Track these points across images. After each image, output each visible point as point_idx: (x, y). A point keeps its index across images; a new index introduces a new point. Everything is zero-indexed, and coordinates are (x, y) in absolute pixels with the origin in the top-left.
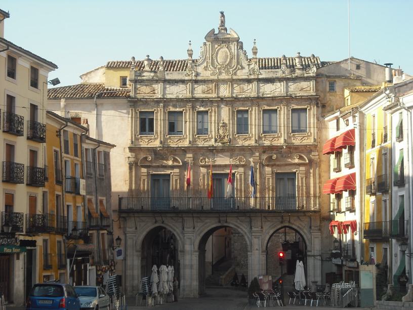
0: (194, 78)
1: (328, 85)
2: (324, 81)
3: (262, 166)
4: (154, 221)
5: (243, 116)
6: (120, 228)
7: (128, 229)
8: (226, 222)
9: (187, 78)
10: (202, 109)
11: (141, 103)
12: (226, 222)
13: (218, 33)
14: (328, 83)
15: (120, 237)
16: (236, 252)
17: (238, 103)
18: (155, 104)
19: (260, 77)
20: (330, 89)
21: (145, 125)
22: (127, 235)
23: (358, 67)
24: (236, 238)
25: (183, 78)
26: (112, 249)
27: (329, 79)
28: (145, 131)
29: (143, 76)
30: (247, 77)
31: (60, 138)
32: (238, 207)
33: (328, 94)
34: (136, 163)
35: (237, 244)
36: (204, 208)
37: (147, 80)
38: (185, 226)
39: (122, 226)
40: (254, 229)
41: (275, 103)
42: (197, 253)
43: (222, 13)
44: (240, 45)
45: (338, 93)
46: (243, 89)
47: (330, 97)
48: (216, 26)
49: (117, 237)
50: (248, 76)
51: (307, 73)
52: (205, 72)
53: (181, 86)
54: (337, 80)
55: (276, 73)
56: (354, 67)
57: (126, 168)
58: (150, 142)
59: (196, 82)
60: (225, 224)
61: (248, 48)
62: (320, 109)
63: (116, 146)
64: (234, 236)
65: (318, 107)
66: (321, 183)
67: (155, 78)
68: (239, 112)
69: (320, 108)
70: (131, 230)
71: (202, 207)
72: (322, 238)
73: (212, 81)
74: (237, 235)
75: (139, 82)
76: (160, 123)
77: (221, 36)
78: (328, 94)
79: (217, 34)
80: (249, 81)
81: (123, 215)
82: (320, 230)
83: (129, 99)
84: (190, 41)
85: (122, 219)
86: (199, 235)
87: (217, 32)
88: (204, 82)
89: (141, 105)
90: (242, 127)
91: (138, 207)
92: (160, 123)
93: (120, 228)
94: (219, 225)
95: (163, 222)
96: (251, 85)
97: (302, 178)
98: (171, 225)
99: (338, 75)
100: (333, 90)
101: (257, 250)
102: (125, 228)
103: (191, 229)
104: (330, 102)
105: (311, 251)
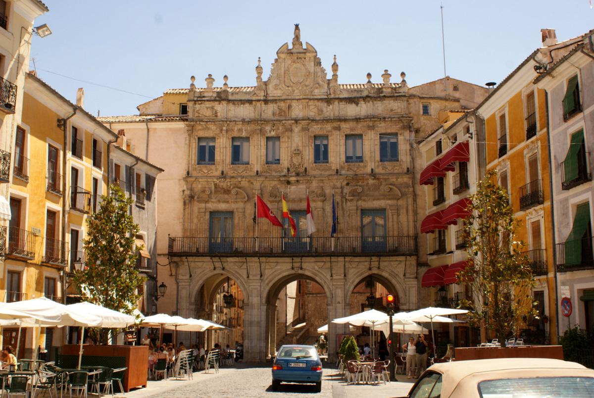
0: (262, 98)
1: (421, 108)
2: (417, 103)
3: (345, 201)
4: (212, 267)
5: (321, 142)
6: (171, 275)
7: (180, 277)
8: (301, 268)
9: (254, 98)
10: (273, 134)
11: (200, 127)
12: (301, 268)
13: (293, 49)
14: (421, 106)
15: (164, 284)
16: (310, 312)
17: (315, 126)
18: (216, 129)
19: (341, 96)
20: (424, 113)
21: (205, 154)
22: (180, 284)
23: (456, 89)
24: (310, 298)
25: (250, 99)
26: (153, 298)
27: (422, 101)
28: (205, 161)
29: (204, 97)
30: (326, 97)
31: (65, 130)
32: (316, 249)
33: (422, 118)
34: (192, 197)
35: (311, 305)
36: (274, 251)
37: (208, 101)
38: (251, 273)
39: (174, 273)
40: (335, 277)
41: (359, 127)
42: (265, 307)
43: (297, 26)
44: (318, 63)
45: (433, 117)
46: (322, 111)
47: (425, 121)
48: (289, 39)
49: (161, 283)
50: (327, 96)
51: (396, 93)
52: (275, 92)
53: (248, 108)
54: (431, 101)
55: (360, 93)
56: (451, 88)
57: (180, 205)
58: (209, 172)
59: (266, 101)
60: (300, 272)
61: (327, 65)
62: (413, 134)
63: (163, 171)
64: (308, 297)
65: (410, 131)
66: (417, 222)
67: (217, 99)
68: (316, 137)
69: (413, 133)
70: (184, 278)
71: (272, 249)
72: (418, 287)
73: (284, 100)
74: (311, 296)
75: (199, 104)
76: (223, 150)
77: (293, 51)
78: (422, 118)
79: (290, 50)
80: (329, 101)
81: (175, 259)
82: (416, 278)
83: (185, 123)
84: (259, 58)
85: (175, 265)
86: (268, 284)
87: (290, 47)
88: (275, 101)
89: (201, 130)
90: (321, 154)
91: (194, 250)
92: (223, 150)
93: (171, 275)
94: (293, 272)
95: (223, 269)
96: (331, 107)
97: (392, 215)
98: (234, 272)
99: (433, 96)
100: (427, 113)
101: (339, 303)
102: (176, 275)
103: (259, 277)
104: (424, 127)
105: (405, 304)
